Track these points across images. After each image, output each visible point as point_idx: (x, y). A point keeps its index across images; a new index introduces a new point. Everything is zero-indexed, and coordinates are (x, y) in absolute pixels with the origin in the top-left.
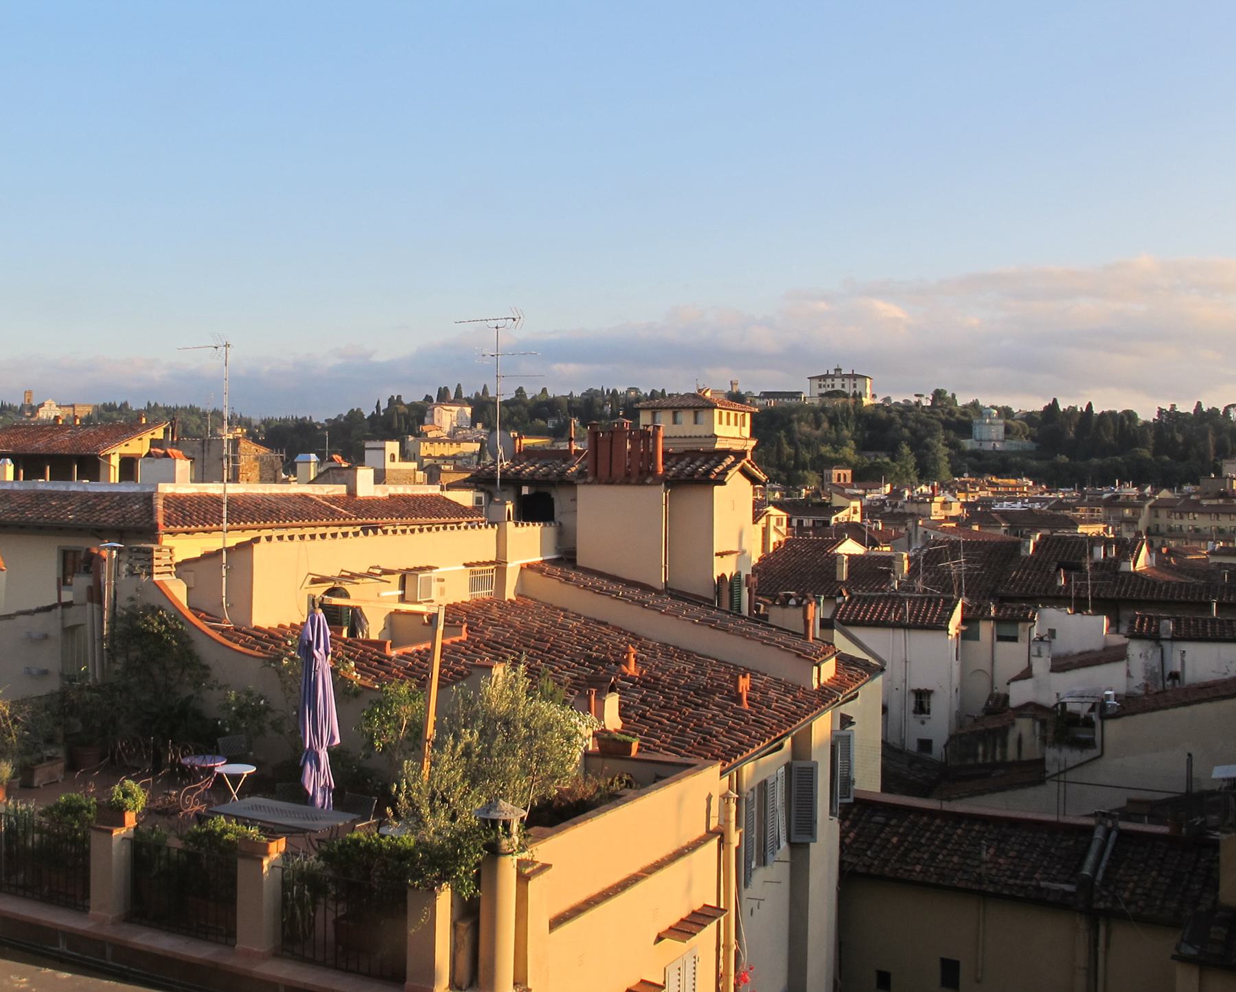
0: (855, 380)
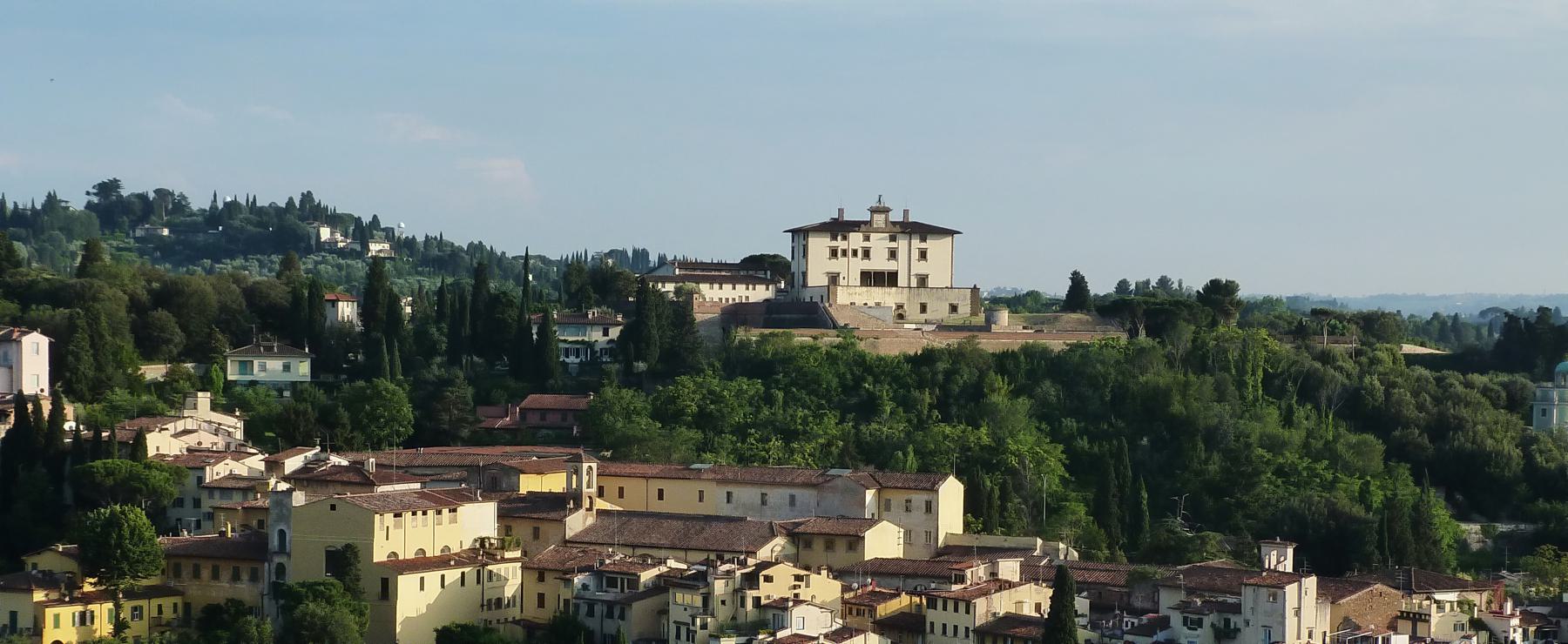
0: (923, 240)
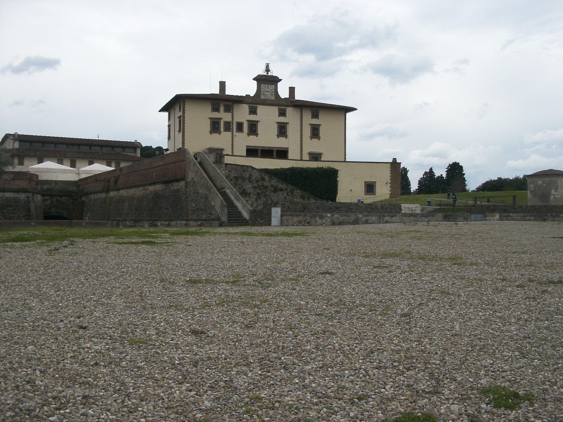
0: (315, 116)
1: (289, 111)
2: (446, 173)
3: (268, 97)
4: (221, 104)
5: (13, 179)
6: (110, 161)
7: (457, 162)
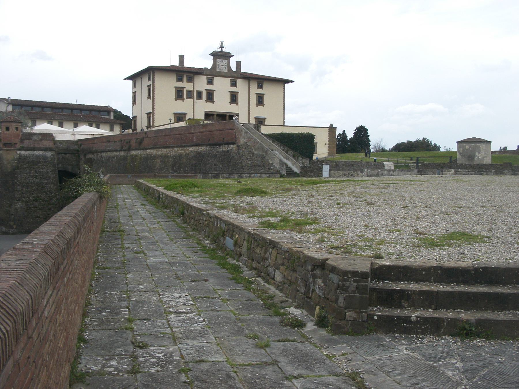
0: (260, 86)
1: (240, 82)
2: (368, 134)
3: (222, 70)
4: (184, 76)
5: (41, 140)
6: (98, 123)
7: (363, 125)
